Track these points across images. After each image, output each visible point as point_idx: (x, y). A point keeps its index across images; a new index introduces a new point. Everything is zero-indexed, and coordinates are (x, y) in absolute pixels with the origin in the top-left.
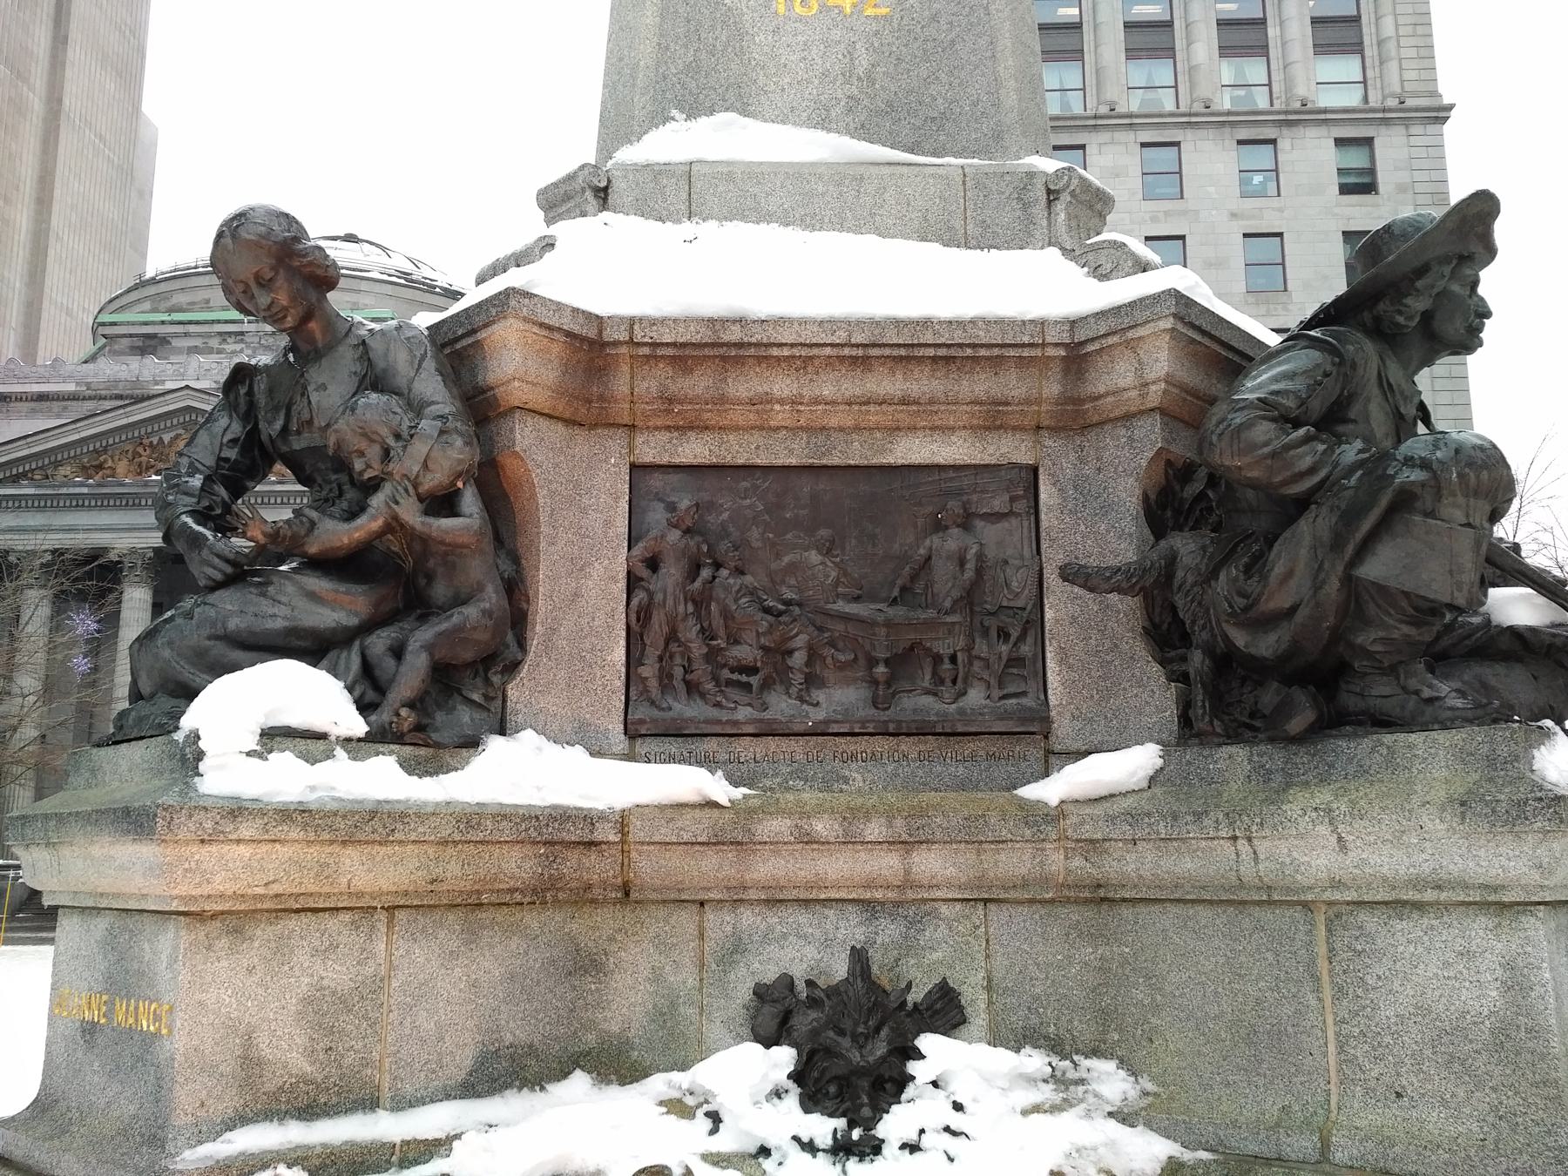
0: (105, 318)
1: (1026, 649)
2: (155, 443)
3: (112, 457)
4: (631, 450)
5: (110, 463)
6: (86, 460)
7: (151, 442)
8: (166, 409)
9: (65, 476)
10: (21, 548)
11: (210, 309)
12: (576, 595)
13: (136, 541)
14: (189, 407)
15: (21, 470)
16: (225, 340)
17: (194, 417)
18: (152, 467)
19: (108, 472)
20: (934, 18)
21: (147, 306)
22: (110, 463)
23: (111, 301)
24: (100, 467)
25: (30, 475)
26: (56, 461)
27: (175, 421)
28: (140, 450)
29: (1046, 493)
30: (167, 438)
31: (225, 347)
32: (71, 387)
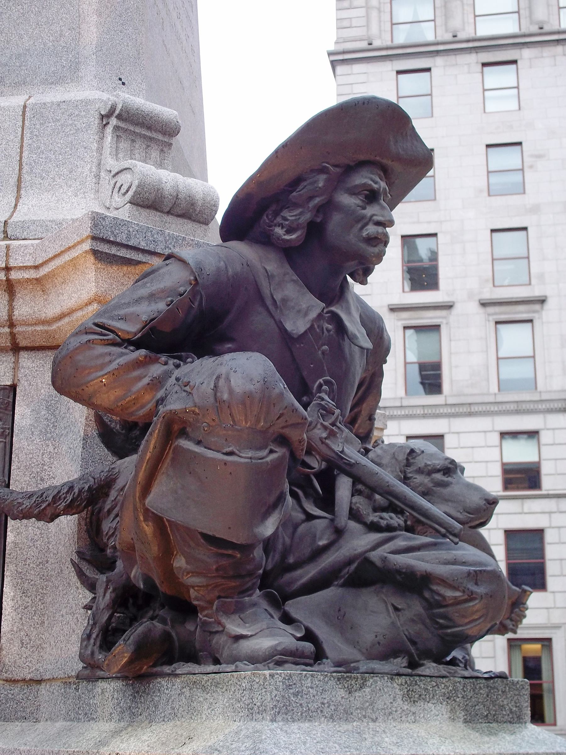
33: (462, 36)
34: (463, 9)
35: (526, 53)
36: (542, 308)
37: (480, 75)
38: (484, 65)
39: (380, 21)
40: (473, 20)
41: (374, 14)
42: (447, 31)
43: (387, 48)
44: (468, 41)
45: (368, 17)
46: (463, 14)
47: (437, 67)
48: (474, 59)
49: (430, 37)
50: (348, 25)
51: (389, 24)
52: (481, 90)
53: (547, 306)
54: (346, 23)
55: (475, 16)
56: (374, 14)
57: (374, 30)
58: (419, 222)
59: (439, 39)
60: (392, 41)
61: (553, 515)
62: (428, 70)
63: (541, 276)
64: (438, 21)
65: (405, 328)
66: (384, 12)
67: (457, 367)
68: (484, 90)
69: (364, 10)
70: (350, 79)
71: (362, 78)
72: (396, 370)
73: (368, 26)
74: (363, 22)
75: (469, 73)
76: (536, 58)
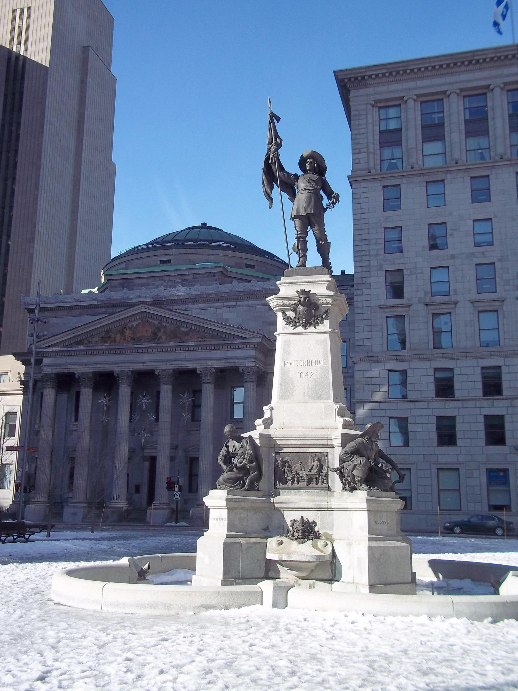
2: (130, 326)
9: (96, 342)
11: (149, 266)
14: (143, 311)
16: (155, 280)
21: (123, 266)
25: (82, 341)
26: (92, 335)
27: (138, 317)
30: (135, 324)
31: (156, 282)
32: (96, 303)
35: (449, 176)
36: (456, 307)
39: (374, 159)
41: (371, 156)
44: (419, 170)
46: (417, 155)
53: (458, 305)
54: (357, 161)
55: (423, 156)
56: (371, 156)
57: (372, 164)
58: (394, 264)
61: (460, 409)
63: (455, 290)
67: (413, 336)
69: (366, 154)
73: (368, 162)
75: (420, 187)
76: (454, 178)
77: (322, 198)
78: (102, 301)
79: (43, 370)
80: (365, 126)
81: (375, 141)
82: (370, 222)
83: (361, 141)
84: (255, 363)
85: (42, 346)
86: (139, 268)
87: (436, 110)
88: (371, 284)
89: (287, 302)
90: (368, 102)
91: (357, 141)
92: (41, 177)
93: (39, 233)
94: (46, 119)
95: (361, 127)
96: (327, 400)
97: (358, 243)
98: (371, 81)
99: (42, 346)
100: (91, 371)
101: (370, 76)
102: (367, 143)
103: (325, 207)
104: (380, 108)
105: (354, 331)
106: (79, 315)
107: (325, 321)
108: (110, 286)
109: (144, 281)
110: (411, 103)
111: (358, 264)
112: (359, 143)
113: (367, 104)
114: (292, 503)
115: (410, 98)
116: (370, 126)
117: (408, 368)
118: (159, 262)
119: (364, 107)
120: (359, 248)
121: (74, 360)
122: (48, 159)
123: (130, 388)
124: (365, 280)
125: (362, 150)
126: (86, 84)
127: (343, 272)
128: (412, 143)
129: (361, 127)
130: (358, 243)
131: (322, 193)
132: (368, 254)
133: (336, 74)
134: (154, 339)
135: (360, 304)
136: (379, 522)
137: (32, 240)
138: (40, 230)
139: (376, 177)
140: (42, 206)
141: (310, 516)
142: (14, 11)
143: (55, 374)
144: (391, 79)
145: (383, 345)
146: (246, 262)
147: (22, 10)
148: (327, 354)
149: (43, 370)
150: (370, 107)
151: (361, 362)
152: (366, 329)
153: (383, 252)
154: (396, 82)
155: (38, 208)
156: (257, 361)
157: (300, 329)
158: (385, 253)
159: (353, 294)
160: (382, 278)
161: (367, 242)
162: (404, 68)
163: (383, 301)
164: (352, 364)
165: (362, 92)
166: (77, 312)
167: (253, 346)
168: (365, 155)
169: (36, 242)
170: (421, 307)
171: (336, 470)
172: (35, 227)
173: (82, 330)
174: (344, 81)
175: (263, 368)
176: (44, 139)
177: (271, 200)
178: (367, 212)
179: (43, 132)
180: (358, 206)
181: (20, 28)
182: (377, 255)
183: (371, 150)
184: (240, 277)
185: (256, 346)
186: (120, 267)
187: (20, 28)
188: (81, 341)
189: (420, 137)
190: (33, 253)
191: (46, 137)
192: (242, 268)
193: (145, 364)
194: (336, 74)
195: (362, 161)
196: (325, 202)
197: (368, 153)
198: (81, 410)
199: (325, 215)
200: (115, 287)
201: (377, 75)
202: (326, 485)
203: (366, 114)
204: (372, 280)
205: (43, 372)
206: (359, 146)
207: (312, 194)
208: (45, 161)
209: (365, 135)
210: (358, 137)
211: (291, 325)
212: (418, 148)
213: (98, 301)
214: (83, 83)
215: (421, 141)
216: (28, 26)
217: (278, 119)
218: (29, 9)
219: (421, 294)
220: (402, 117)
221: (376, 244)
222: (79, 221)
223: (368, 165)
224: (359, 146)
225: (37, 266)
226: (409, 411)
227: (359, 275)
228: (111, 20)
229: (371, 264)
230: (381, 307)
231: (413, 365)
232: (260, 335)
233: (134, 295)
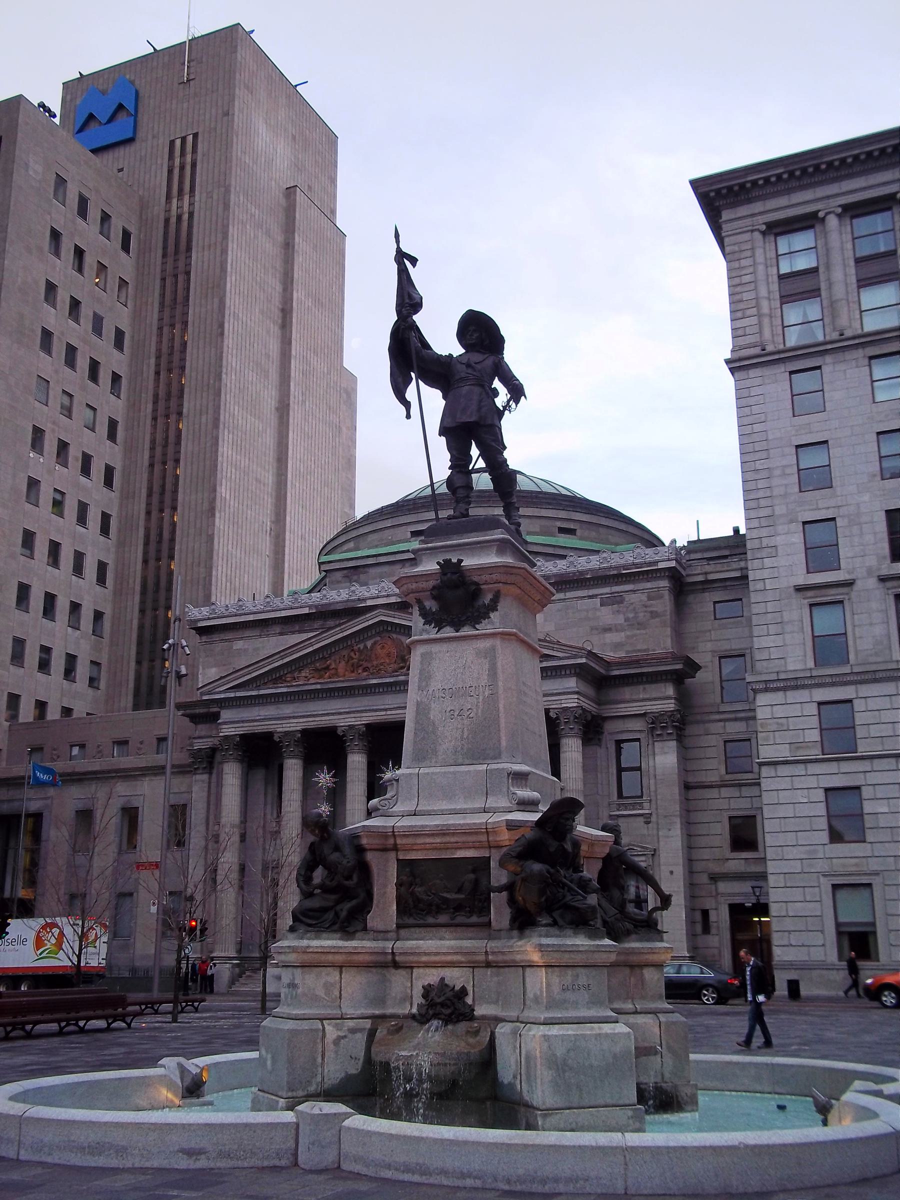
0: (324, 559)
1: (486, 904)
2: (362, 648)
3: (335, 661)
4: (397, 855)
5: (333, 666)
6: (318, 665)
7: (359, 648)
8: (367, 624)
9: (306, 677)
10: (281, 730)
11: (393, 543)
12: (385, 893)
13: (353, 720)
15: (278, 675)
16: (403, 567)
17: (385, 628)
18: (361, 666)
19: (333, 672)
20: (485, 719)
21: (351, 545)
22: (333, 666)
23: (328, 543)
24: (327, 668)
28: (352, 654)
29: (492, 864)
32: (306, 611)
33: (848, 333)
34: (849, 307)
37: (867, 368)
38: (871, 358)
39: (772, 326)
40: (858, 316)
41: (766, 321)
42: (834, 330)
43: (779, 352)
45: (760, 324)
47: (827, 364)
48: (860, 354)
49: (820, 338)
50: (742, 334)
51: (780, 328)
52: (869, 382)
54: (740, 332)
55: (861, 312)
56: (766, 321)
57: (767, 334)
59: (828, 338)
60: (785, 345)
62: (819, 368)
64: (827, 320)
65: (811, 605)
66: (775, 317)
68: (873, 381)
70: (748, 383)
71: (758, 381)
72: (804, 644)
73: (761, 332)
74: (756, 329)
75: (857, 367)
77: (495, 393)
78: (316, 607)
79: (222, 731)
80: (751, 270)
81: (771, 294)
82: (770, 437)
83: (745, 296)
84: (576, 700)
85: (217, 690)
86: (377, 546)
87: (880, 229)
88: (779, 548)
89: (424, 583)
90: (754, 228)
91: (738, 297)
92: (222, 407)
93: (223, 501)
94: (227, 312)
95: (744, 272)
96: (495, 758)
97: (750, 476)
98: (755, 193)
99: (217, 690)
100: (298, 728)
101: (754, 183)
102: (757, 299)
103: (502, 409)
104: (777, 235)
105: (751, 636)
106: (281, 634)
107: (492, 615)
108: (329, 581)
109: (386, 569)
110: (832, 222)
111: (753, 514)
112: (741, 301)
113: (752, 231)
114: (426, 954)
115: (830, 213)
116: (761, 268)
117: (854, 696)
118: (409, 535)
119: (747, 236)
120: (752, 486)
121: (269, 711)
122: (233, 377)
123: (365, 756)
124: (765, 542)
125: (748, 312)
126: (293, 247)
127: (736, 530)
128: (839, 291)
129: (744, 272)
130: (750, 476)
131: (497, 384)
132: (768, 494)
133: (697, 185)
134: (402, 668)
135: (760, 586)
136: (570, 987)
137: (212, 511)
138: (224, 495)
139: (777, 357)
140: (225, 455)
141: (456, 977)
142: (172, 143)
143: (241, 736)
144: (794, 183)
145: (805, 656)
146: (559, 524)
147: (184, 140)
148: (495, 674)
149: (222, 731)
150: (757, 235)
151: (766, 690)
152: (773, 629)
153: (797, 490)
154: (802, 188)
155: (220, 459)
156: (581, 698)
157: (448, 632)
158: (801, 491)
159: (747, 568)
160: (796, 535)
161: (764, 474)
162: (815, 162)
163: (802, 579)
164: (751, 693)
165: (743, 211)
166: (277, 629)
167: (573, 672)
168: (754, 320)
169: (217, 515)
170: (872, 583)
171: (500, 890)
172: (215, 490)
173: (282, 658)
174: (709, 195)
175: (594, 710)
176: (225, 343)
177: (407, 405)
178: (763, 420)
179: (222, 334)
180: (747, 410)
181: (182, 168)
182: (785, 496)
183: (765, 310)
184: (550, 551)
185: (578, 671)
186: (345, 547)
187: (182, 168)
188: (280, 677)
189: (853, 280)
190: (213, 534)
191: (229, 341)
192: (553, 535)
193: (389, 712)
194: (697, 185)
195: (748, 331)
196: (502, 397)
197: (760, 315)
198: (285, 796)
199: (504, 422)
200: (339, 582)
201: (767, 180)
202: (485, 919)
203: (753, 249)
204: (779, 540)
205: (221, 734)
206: (741, 306)
207: (472, 387)
208: (229, 380)
209: (753, 284)
210: (739, 289)
211: (433, 625)
212: (850, 299)
213: (310, 607)
214: (288, 247)
215: (855, 286)
216: (194, 165)
217: (414, 261)
218: (196, 136)
219: (872, 561)
220: (819, 247)
221: (784, 475)
222: (289, 476)
223: (761, 337)
224: (741, 306)
225: (220, 555)
226: (862, 775)
227: (755, 534)
228: (332, 140)
229: (776, 513)
230: (799, 589)
231: (866, 690)
232: (583, 651)
233: (367, 595)
